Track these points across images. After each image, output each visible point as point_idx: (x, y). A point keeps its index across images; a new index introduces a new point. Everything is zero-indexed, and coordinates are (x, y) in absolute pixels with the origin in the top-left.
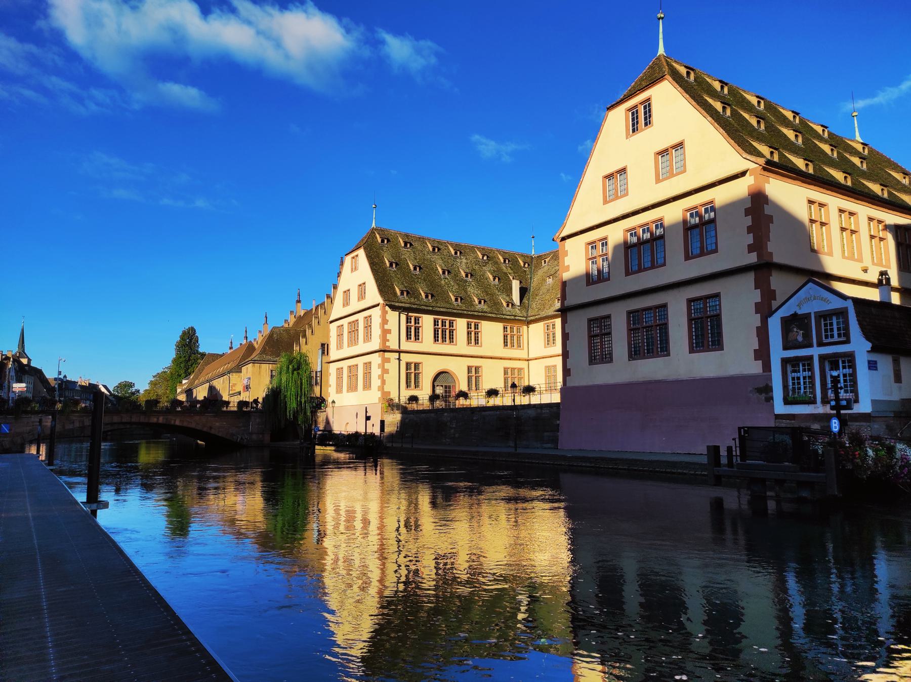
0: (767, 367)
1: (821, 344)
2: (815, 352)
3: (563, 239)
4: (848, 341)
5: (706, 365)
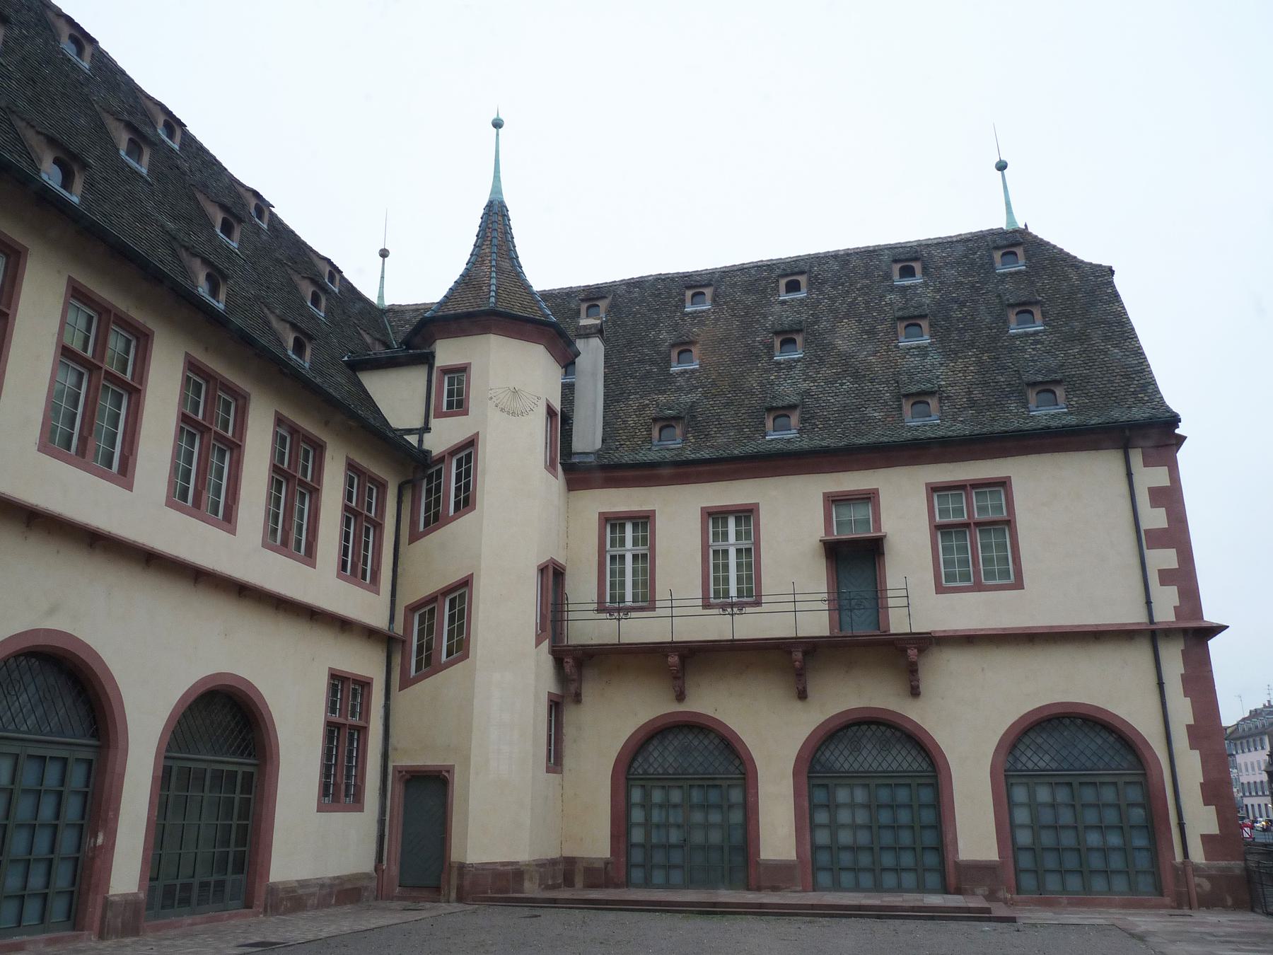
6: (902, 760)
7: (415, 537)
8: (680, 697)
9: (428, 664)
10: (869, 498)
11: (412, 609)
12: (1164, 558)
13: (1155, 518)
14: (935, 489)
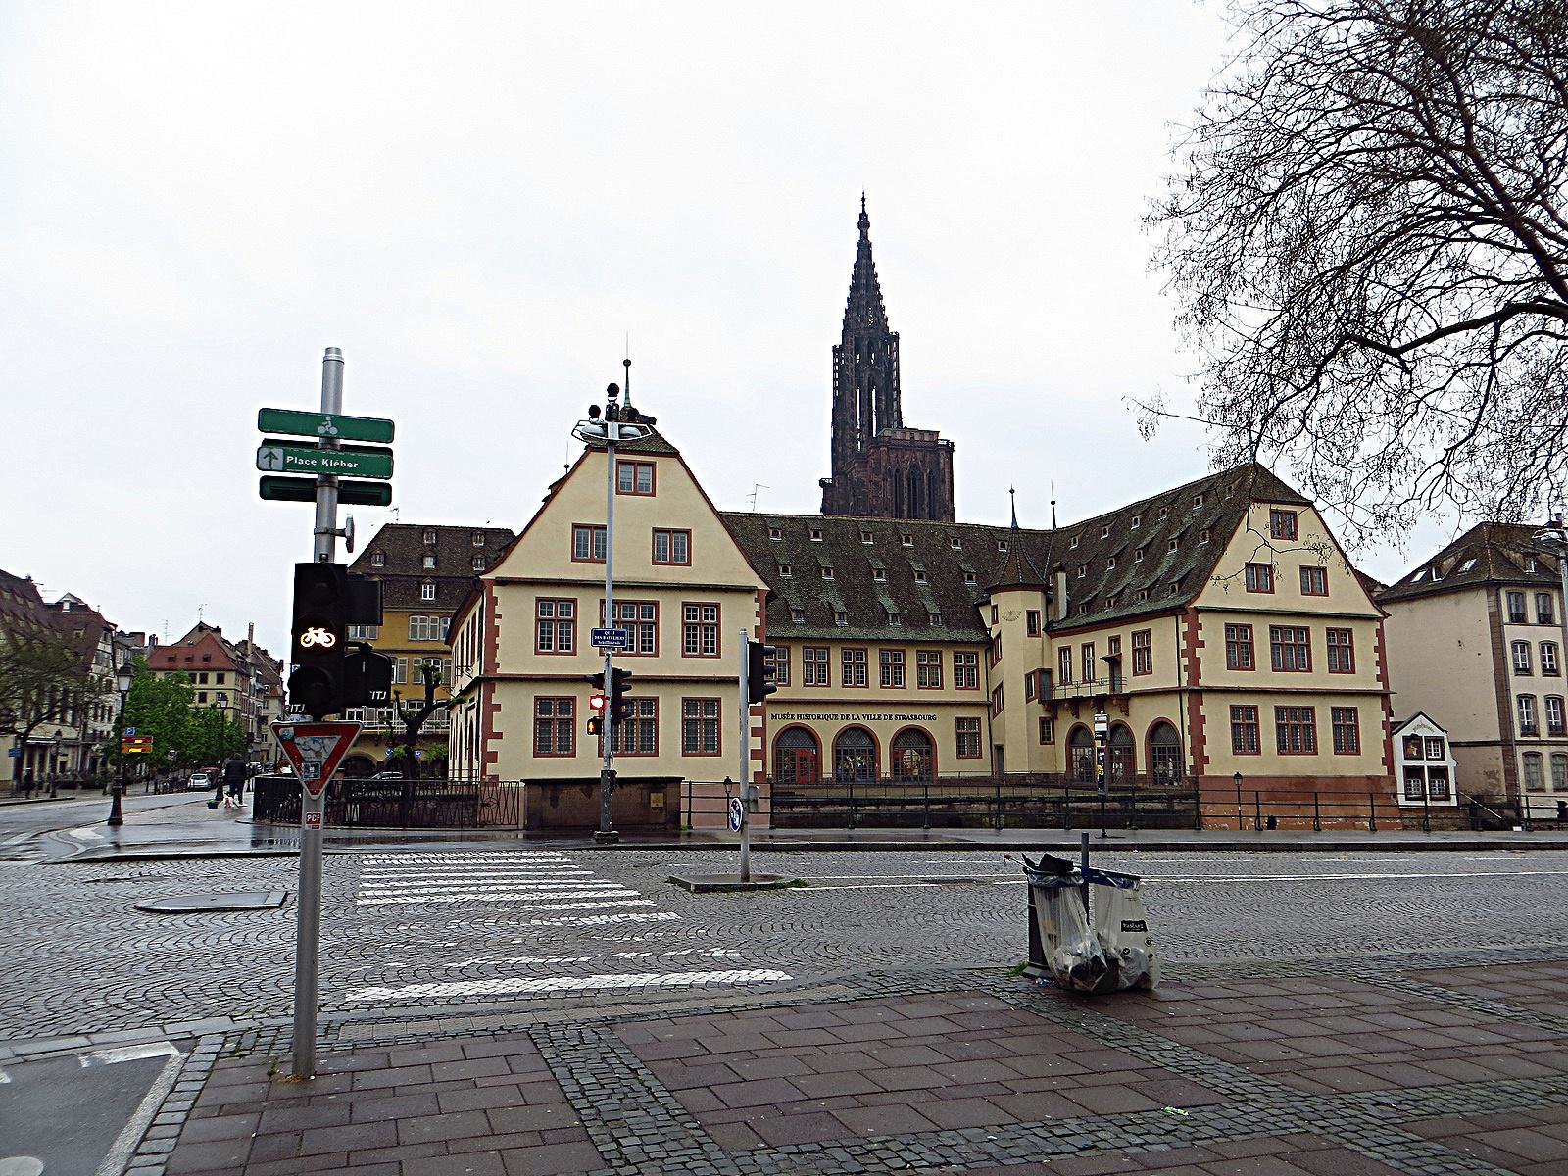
0: (1391, 771)
1: (1428, 759)
2: (1425, 764)
3: (1198, 610)
4: (1443, 759)
5: (1348, 766)
7: (993, 666)
8: (1078, 717)
9: (1000, 710)
11: (994, 692)
13: (1183, 645)
14: (1134, 634)
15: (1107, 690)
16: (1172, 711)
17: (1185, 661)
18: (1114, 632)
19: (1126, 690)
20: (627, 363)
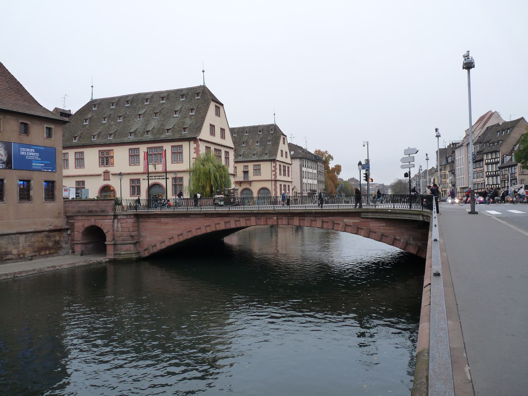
6: (266, 191)
10: (247, 166)
12: (274, 173)
13: (273, 169)
15: (242, 180)
16: (268, 185)
17: (274, 173)
18: (246, 164)
19: (250, 179)
20: (203, 71)
